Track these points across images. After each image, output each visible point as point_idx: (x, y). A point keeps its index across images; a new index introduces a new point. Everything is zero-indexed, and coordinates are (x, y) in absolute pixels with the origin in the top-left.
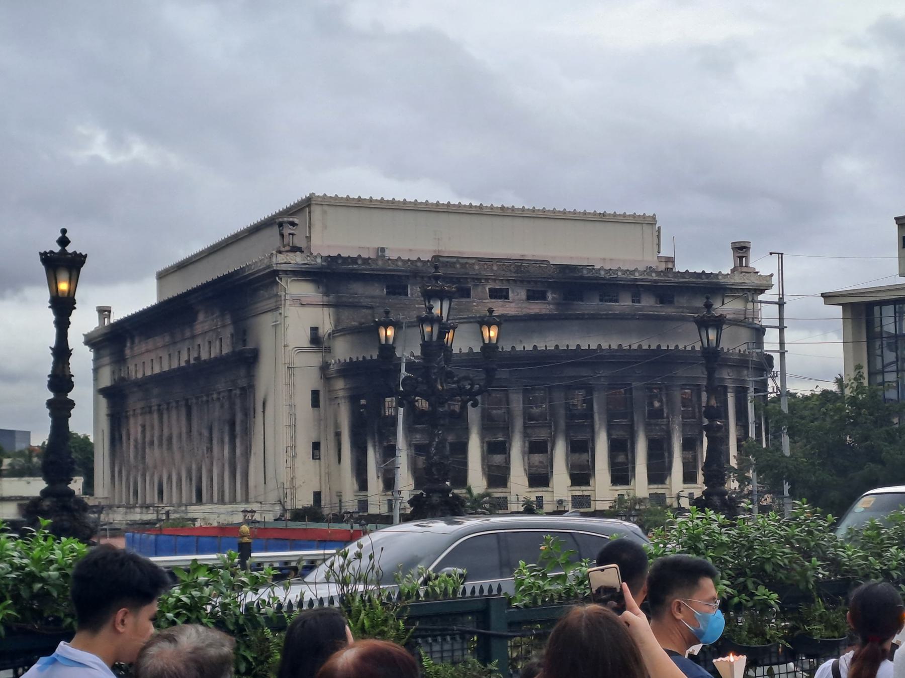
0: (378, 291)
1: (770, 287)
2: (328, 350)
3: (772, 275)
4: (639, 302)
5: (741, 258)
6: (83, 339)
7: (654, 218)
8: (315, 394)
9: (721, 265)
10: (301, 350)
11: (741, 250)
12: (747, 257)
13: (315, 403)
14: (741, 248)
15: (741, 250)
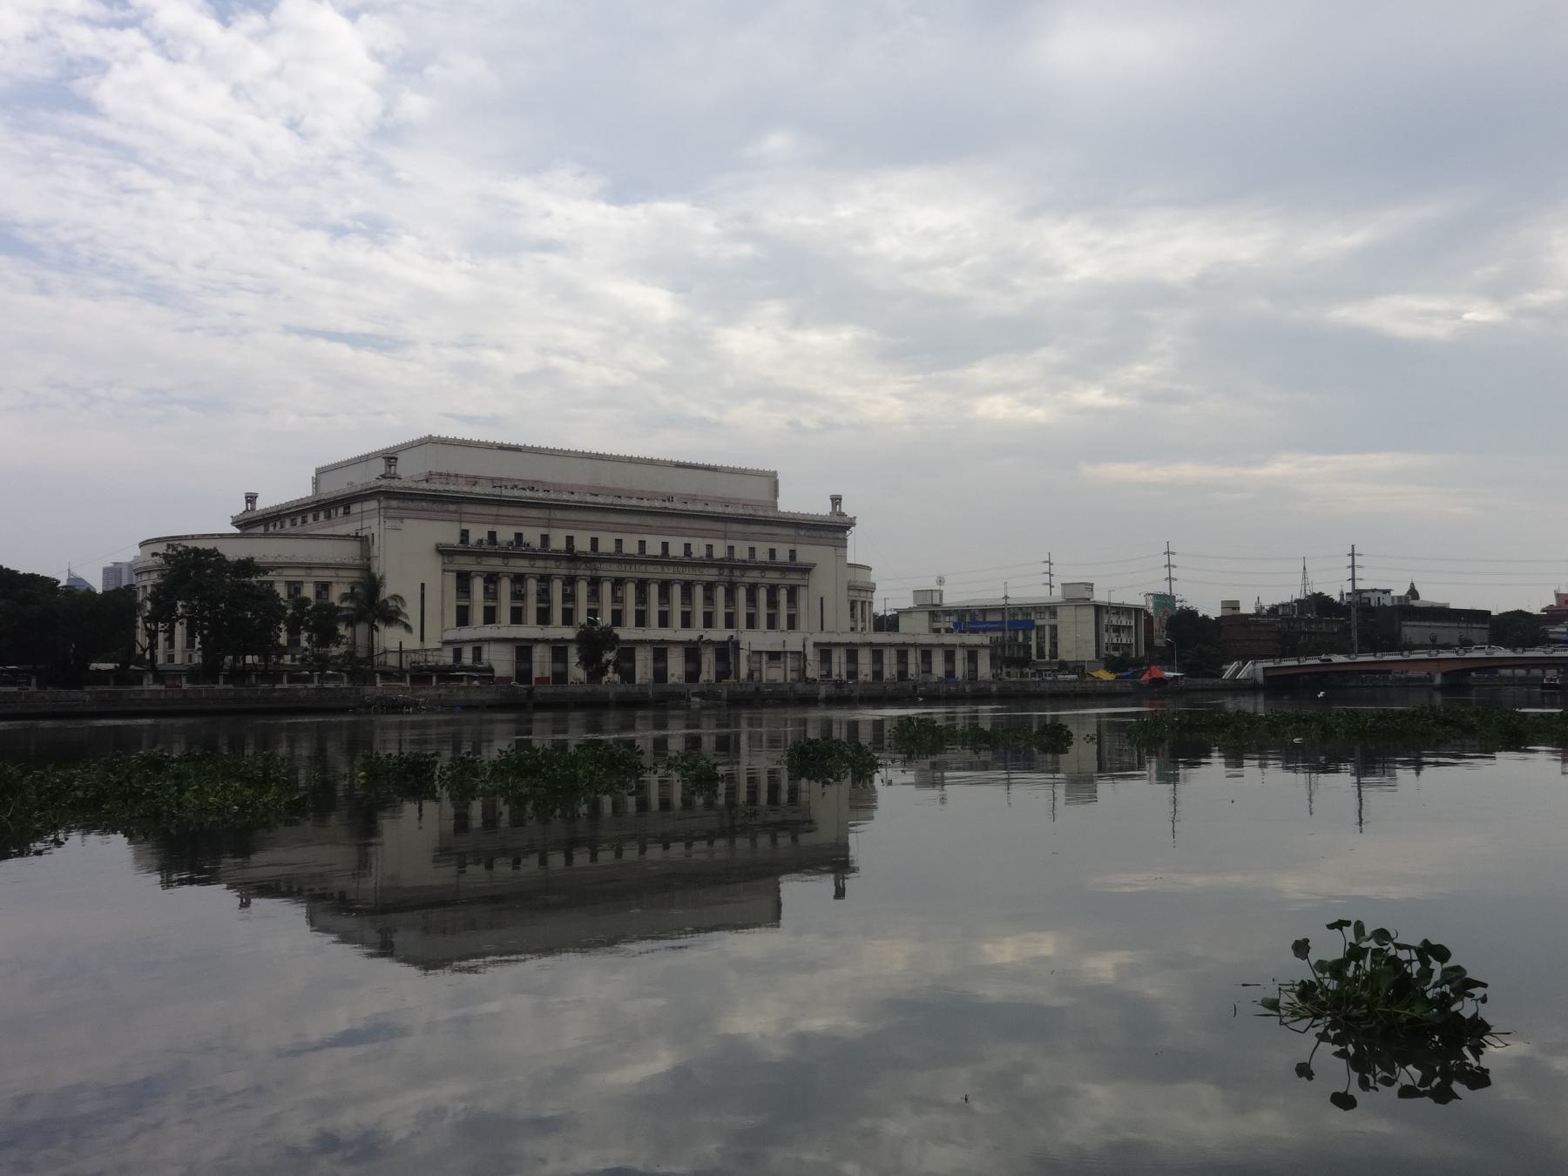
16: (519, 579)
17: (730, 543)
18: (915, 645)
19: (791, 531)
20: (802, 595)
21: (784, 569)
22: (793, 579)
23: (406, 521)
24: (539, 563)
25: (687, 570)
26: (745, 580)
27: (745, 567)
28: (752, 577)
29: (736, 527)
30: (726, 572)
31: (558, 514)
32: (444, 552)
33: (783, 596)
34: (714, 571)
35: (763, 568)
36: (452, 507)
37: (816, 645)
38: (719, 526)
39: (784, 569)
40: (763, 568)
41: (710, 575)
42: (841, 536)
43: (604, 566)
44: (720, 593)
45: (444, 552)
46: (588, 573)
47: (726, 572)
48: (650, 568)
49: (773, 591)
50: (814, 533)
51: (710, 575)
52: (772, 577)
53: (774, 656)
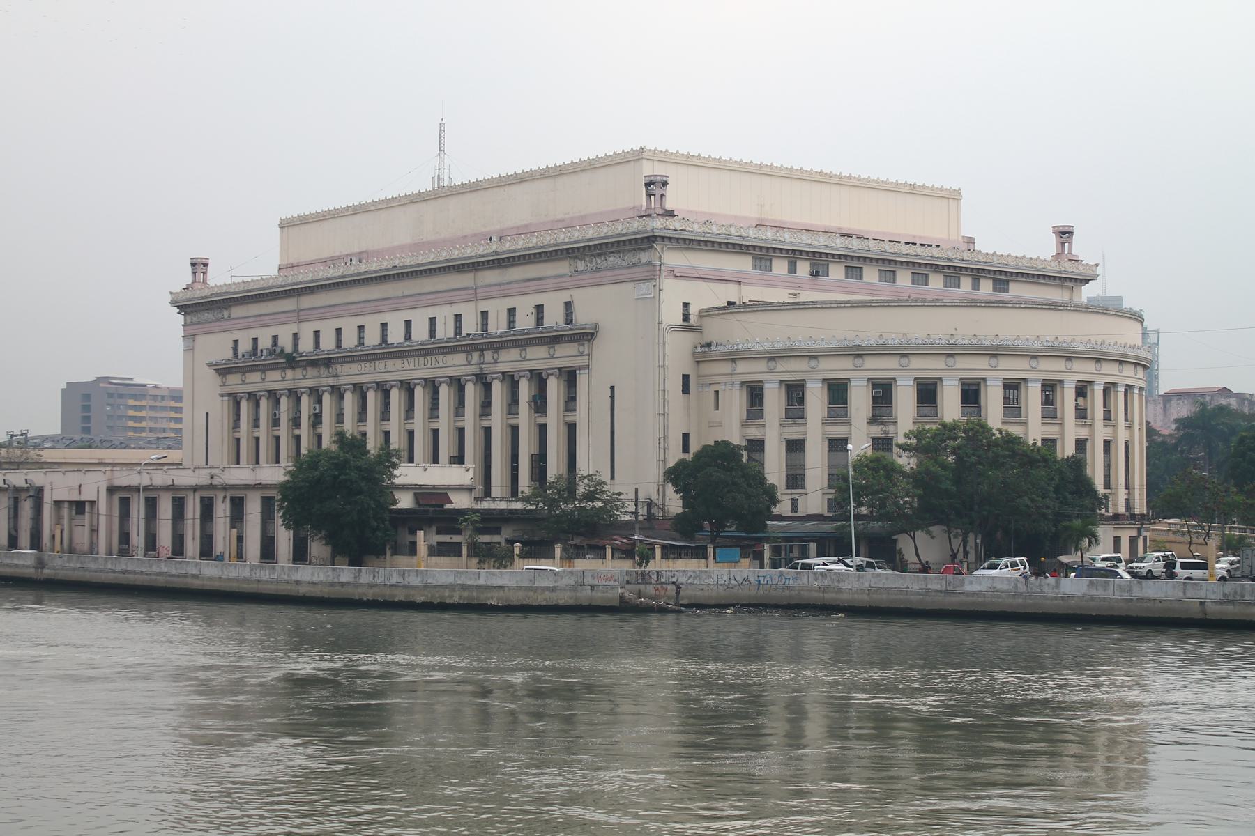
0: (743, 264)
1: (1095, 277)
2: (698, 329)
3: (1097, 265)
4: (1006, 290)
5: (1063, 244)
6: (169, 298)
7: (958, 192)
8: (686, 378)
9: (1042, 250)
10: (674, 328)
11: (1064, 234)
12: (1070, 243)
13: (686, 390)
14: (1064, 233)
15: (1064, 234)
16: (274, 397)
17: (483, 306)
18: (225, 488)
19: (562, 267)
20: (582, 379)
21: (555, 340)
22: (566, 355)
25: (431, 361)
26: (502, 368)
27: (498, 346)
28: (509, 360)
29: (490, 277)
31: (307, 302)
32: (223, 371)
33: (554, 389)
34: (460, 358)
35: (523, 342)
36: (226, 314)
37: (112, 490)
38: (466, 280)
39: (555, 340)
40: (523, 342)
41: (457, 364)
42: (644, 257)
43: (346, 368)
44: (472, 393)
45: (223, 371)
46: (331, 381)
47: (476, 355)
49: (539, 380)
51: (457, 364)
52: (537, 357)
53: (79, 507)
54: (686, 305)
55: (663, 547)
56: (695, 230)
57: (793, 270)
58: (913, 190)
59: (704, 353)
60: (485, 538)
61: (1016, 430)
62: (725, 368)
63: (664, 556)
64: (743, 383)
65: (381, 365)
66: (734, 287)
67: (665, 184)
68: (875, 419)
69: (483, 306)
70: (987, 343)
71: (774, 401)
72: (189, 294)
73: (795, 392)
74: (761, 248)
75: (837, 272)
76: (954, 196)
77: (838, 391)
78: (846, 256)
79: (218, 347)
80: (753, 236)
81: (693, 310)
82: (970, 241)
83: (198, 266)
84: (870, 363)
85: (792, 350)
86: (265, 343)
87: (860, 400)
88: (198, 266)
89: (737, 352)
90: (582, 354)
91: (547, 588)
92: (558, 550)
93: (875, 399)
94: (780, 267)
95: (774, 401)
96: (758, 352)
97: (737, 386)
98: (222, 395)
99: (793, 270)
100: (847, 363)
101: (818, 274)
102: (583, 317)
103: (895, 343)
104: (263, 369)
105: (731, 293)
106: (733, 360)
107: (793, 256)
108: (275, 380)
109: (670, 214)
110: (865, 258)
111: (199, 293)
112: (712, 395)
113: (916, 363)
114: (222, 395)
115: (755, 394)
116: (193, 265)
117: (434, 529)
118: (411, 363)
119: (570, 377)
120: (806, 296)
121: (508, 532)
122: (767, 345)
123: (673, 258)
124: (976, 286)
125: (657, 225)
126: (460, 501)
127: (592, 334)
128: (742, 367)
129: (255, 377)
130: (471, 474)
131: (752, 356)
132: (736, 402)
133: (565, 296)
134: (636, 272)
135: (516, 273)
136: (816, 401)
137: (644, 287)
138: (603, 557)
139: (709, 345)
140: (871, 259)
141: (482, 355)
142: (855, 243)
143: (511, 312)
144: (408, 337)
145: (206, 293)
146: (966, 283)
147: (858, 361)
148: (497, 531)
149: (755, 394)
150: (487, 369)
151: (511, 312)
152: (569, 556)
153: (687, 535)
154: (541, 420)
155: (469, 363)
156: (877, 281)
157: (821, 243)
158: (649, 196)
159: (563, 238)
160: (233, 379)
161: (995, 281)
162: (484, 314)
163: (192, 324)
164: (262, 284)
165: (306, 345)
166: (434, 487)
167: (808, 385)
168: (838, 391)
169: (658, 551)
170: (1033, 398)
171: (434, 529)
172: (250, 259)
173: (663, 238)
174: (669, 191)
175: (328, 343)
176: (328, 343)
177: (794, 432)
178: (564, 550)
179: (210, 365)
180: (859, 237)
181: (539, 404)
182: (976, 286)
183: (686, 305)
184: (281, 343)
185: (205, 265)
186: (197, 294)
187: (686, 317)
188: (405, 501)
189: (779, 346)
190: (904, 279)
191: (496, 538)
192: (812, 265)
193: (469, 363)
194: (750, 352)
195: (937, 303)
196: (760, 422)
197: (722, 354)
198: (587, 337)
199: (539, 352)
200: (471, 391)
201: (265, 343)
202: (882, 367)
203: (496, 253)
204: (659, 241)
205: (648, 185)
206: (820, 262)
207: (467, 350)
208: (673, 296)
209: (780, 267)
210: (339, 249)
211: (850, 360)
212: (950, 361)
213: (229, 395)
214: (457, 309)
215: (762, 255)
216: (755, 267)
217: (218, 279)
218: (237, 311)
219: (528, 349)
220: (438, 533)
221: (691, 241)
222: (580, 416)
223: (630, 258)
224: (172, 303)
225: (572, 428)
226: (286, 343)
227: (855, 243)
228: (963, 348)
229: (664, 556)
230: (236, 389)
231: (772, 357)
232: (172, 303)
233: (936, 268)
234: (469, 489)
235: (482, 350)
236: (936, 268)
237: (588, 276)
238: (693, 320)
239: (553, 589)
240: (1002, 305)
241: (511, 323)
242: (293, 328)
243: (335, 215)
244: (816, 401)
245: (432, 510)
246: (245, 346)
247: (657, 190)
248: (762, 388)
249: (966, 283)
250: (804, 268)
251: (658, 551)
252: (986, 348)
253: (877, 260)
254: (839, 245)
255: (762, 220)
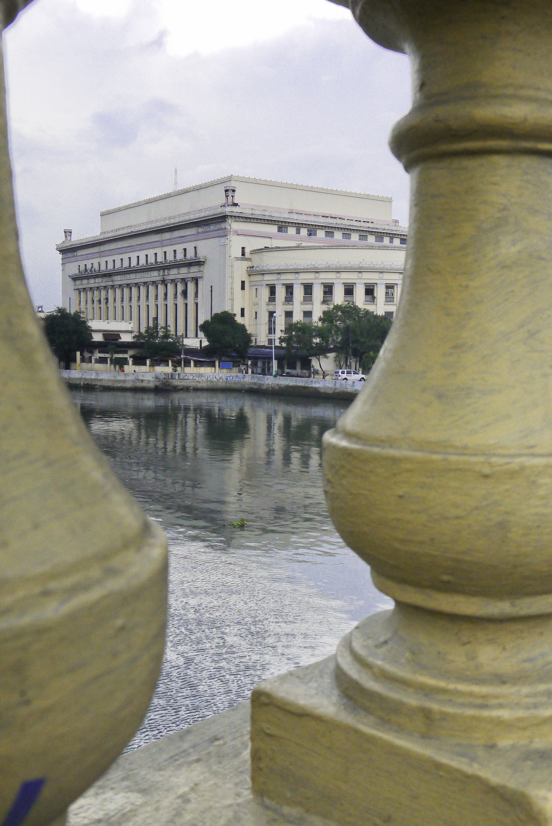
0: (273, 229)
8: (243, 283)
10: (237, 259)
13: (243, 288)
19: (192, 231)
21: (189, 265)
23: (66, 264)
24: (97, 280)
25: (145, 274)
26: (171, 277)
29: (167, 236)
30: (162, 271)
32: (75, 279)
33: (191, 287)
34: (155, 273)
35: (178, 265)
36: (75, 254)
40: (178, 265)
41: (155, 276)
42: (223, 225)
45: (75, 279)
46: (111, 283)
47: (162, 271)
48: (133, 276)
50: (206, 229)
54: (243, 248)
55: (195, 361)
56: (248, 212)
57: (298, 232)
58: (367, 197)
59: (252, 272)
60: (121, 356)
61: (371, 308)
62: (259, 278)
63: (195, 366)
64: (267, 285)
65: (128, 276)
66: (269, 240)
67: (234, 191)
68: (324, 302)
69: (165, 249)
70: (378, 266)
71: (281, 293)
72: (62, 246)
73: (289, 288)
74: (282, 222)
75: (321, 234)
76: (390, 201)
77: (308, 289)
78: (325, 226)
79: (73, 269)
80: (277, 215)
81: (247, 251)
82: (396, 222)
83: (68, 233)
84: (322, 276)
85: (288, 270)
86: (89, 267)
87: (318, 293)
88: (68, 233)
89: (264, 271)
90: (200, 271)
91: (122, 381)
92: (148, 362)
93: (325, 293)
94: (292, 231)
95: (281, 293)
96: (273, 270)
97: (265, 286)
98: (75, 290)
99: (298, 232)
100: (312, 276)
101: (310, 235)
102: (201, 254)
103: (334, 266)
104: (88, 278)
105: (267, 243)
106: (263, 274)
107: (298, 226)
108: (92, 283)
109: (236, 205)
110: (335, 228)
111: (68, 244)
112: (254, 291)
113: (344, 275)
114: (75, 290)
115: (272, 290)
116: (65, 232)
117: (97, 351)
118: (139, 275)
119: (196, 280)
120: (304, 244)
121: (131, 352)
122: (276, 267)
123: (235, 226)
124: (391, 242)
125: (228, 210)
126: (126, 338)
127: (204, 262)
128: (267, 277)
129: (85, 281)
130: (132, 325)
131: (271, 273)
132: (265, 293)
133: (193, 244)
134: (220, 233)
135: (177, 234)
136: (298, 293)
137: (223, 240)
138: (168, 365)
139: (253, 267)
140: (338, 228)
141: (164, 272)
142: (330, 220)
143: (175, 251)
144: (138, 264)
145: (71, 243)
146: (386, 240)
147: (317, 275)
148: (126, 352)
149: (272, 290)
150: (166, 278)
151: (175, 251)
152: (152, 365)
153: (205, 357)
154: (185, 302)
155: (159, 275)
156: (324, 236)
157: (312, 220)
158: (227, 196)
159: (192, 217)
160: (78, 282)
161: (401, 239)
162: (165, 252)
163: (64, 258)
164: (87, 240)
165: (103, 268)
166: (112, 331)
167: (295, 286)
168: (308, 289)
169: (192, 363)
170: (380, 292)
171: (97, 351)
172: (88, 230)
173: (231, 216)
174: (236, 194)
175: (110, 266)
176: (110, 266)
177: (288, 308)
178: (150, 362)
179: (69, 276)
180: (339, 218)
181: (185, 294)
182: (391, 242)
183: (243, 248)
184: (94, 267)
185: (71, 232)
186: (68, 244)
187: (243, 254)
188: (98, 338)
189: (282, 268)
190: (355, 237)
191: (125, 356)
192: (308, 231)
193: (159, 275)
194: (270, 270)
195: (354, 247)
196: (274, 303)
197: (258, 271)
198: (200, 263)
199: (184, 270)
200: (160, 286)
201: (89, 267)
202: (328, 278)
203: (168, 225)
204: (229, 218)
205: (227, 191)
206: (312, 230)
207: (158, 269)
208: (235, 244)
209: (292, 231)
210: (121, 225)
211: (314, 274)
212: (360, 275)
213: (78, 289)
214: (156, 250)
215: (282, 226)
216: (279, 231)
217: (77, 238)
218: (80, 253)
219: (181, 269)
220: (99, 352)
221: (246, 218)
222: (199, 300)
223: (218, 226)
224: (57, 249)
225: (197, 304)
226: (96, 266)
227: (330, 220)
228: (366, 268)
229: (195, 366)
230: (80, 287)
231: (279, 273)
232: (57, 249)
233: (371, 233)
234: (131, 332)
235: (164, 269)
236: (371, 233)
237: (202, 235)
238: (247, 255)
239: (124, 381)
240: (379, 248)
241: (175, 257)
242: (97, 260)
243: (119, 210)
244: (298, 293)
245: (111, 341)
246: (82, 268)
247: (230, 194)
248: (275, 287)
249: (386, 240)
250: (304, 232)
251: (192, 363)
252: (377, 269)
253: (341, 228)
254: (322, 221)
255: (292, 210)
